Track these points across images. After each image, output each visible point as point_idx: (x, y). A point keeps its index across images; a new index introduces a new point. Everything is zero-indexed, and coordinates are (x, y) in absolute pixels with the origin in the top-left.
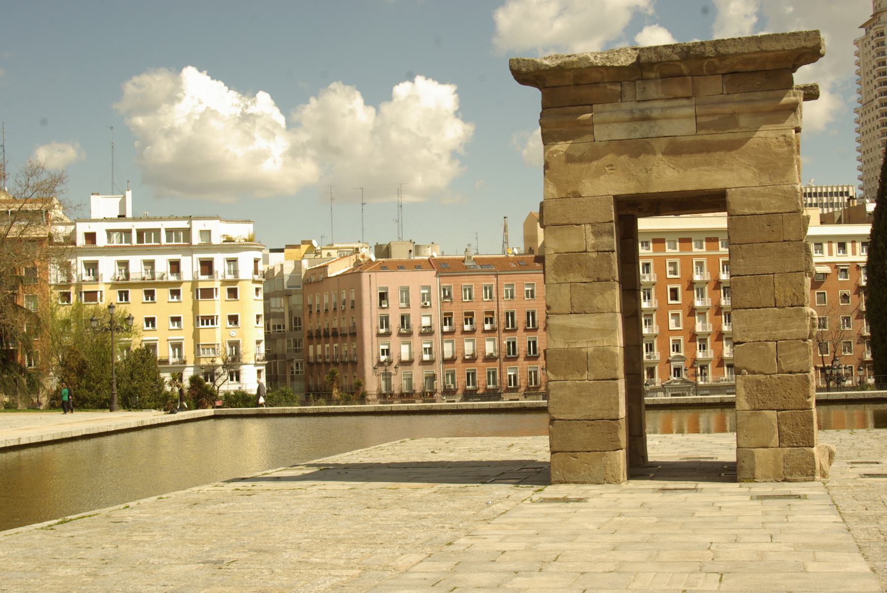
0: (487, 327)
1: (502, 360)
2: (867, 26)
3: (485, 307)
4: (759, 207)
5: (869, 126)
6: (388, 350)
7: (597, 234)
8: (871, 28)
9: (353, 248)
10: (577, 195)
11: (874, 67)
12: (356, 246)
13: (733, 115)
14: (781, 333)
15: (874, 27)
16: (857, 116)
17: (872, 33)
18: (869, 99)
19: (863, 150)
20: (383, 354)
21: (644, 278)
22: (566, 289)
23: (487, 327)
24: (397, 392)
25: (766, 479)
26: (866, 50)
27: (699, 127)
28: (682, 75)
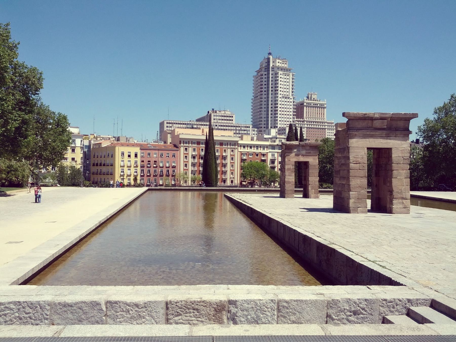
0: (155, 166)
1: (159, 176)
2: (258, 72)
3: (154, 160)
4: (313, 164)
5: (256, 105)
6: (123, 171)
7: (292, 166)
8: (259, 73)
9: (108, 138)
10: (290, 161)
11: (259, 86)
12: (109, 137)
13: (310, 152)
14: (315, 180)
15: (260, 72)
16: (252, 101)
17: (259, 74)
18: (256, 96)
19: (253, 112)
20: (122, 172)
21: (202, 153)
22: (288, 173)
23: (155, 166)
24: (126, 184)
25: (313, 198)
26: (256, 80)
27: (306, 153)
28: (304, 146)
